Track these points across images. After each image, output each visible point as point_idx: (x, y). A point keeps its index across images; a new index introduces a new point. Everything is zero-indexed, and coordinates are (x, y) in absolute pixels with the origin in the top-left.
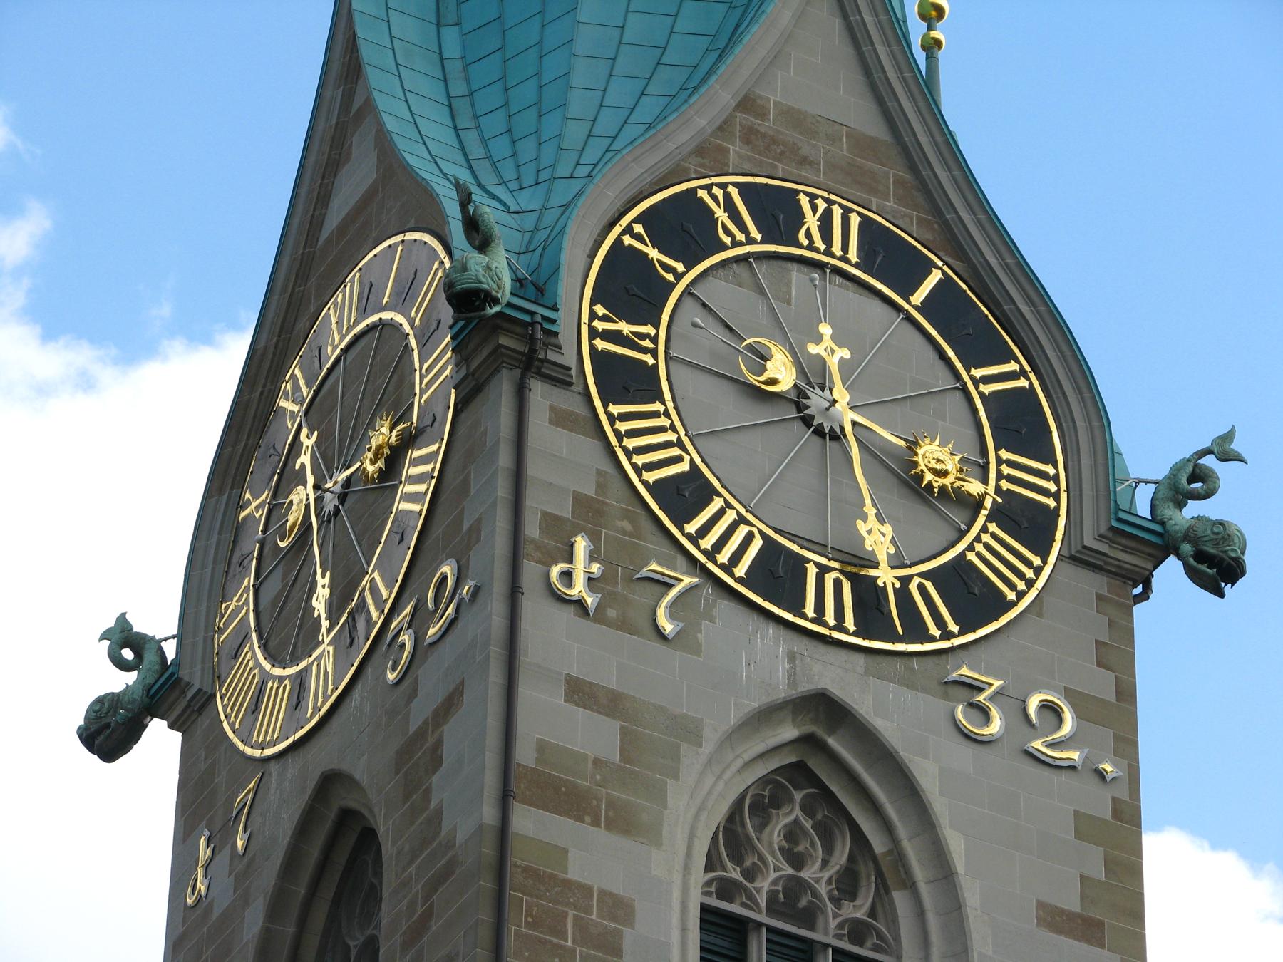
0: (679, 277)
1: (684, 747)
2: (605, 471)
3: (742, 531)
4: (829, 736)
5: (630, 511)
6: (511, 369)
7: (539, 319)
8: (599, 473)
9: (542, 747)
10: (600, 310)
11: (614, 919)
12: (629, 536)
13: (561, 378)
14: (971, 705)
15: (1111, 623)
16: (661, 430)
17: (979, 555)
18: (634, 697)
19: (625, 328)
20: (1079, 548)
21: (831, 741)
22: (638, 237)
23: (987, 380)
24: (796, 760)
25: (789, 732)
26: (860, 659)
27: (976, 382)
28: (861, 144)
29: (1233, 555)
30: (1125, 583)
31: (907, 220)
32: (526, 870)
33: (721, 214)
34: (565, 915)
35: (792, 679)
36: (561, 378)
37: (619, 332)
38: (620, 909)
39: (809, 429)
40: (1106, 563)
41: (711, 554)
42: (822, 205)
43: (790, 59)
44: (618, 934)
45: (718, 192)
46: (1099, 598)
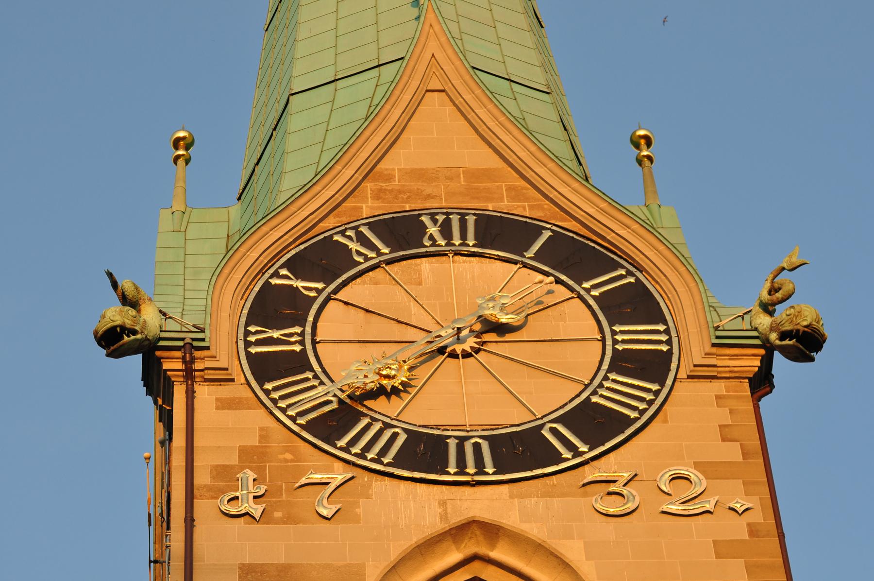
2: (266, 427)
3: (388, 434)
4: (492, 551)
5: (287, 446)
6: (181, 384)
7: (187, 341)
12: (291, 462)
14: (609, 493)
15: (731, 411)
18: (301, 564)
19: (276, 334)
20: (692, 368)
21: (494, 554)
24: (470, 578)
25: (455, 557)
26: (505, 488)
27: (588, 291)
29: (805, 323)
30: (741, 382)
33: (353, 246)
35: (444, 517)
37: (272, 338)
39: (444, 355)
40: (718, 372)
41: (362, 455)
42: (441, 218)
43: (411, 141)
46: (718, 397)
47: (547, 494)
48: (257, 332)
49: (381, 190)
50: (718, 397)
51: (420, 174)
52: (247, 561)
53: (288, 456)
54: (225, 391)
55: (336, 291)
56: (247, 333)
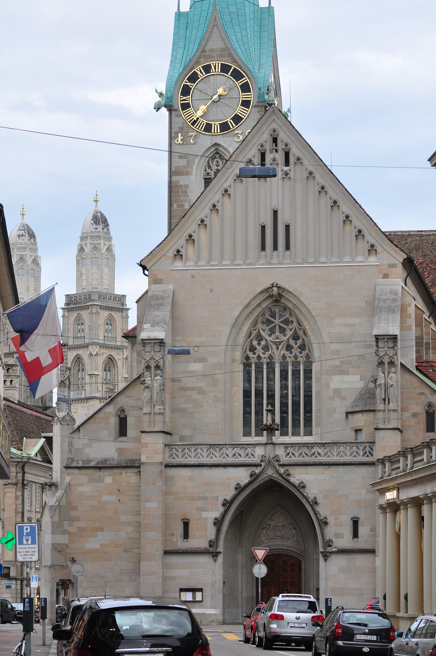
0: (193, 86)
3: (203, 123)
9: (176, 167)
10: (181, 96)
11: (186, 188)
16: (191, 112)
19: (185, 98)
21: (219, 148)
22: (187, 82)
23: (240, 83)
25: (213, 149)
26: (221, 136)
32: (174, 186)
35: (211, 143)
36: (176, 110)
38: (187, 186)
42: (214, 64)
45: (199, 69)
47: (228, 137)
48: (182, 98)
49: (205, 55)
51: (212, 50)
54: (177, 113)
56: (180, 98)
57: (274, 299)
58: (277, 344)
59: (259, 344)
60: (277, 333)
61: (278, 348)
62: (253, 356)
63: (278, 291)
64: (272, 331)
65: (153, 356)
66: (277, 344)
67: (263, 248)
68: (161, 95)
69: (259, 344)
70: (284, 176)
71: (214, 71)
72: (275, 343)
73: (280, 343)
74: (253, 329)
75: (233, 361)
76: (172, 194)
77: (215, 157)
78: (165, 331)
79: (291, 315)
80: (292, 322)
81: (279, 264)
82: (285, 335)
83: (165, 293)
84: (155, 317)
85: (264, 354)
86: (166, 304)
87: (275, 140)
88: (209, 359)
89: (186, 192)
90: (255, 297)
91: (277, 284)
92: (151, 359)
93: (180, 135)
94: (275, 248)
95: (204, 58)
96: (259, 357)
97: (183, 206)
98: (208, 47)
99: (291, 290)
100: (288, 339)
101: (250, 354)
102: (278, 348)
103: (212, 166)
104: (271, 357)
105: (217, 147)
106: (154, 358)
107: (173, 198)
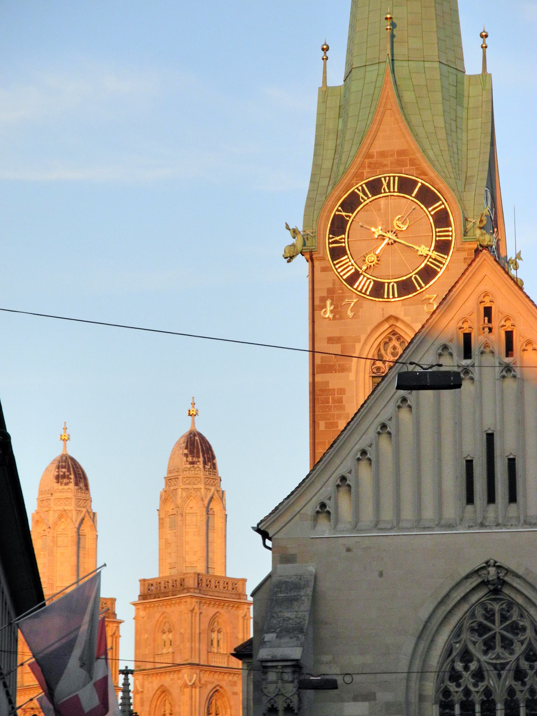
0: (350, 217)
1: (357, 344)
8: (334, 280)
10: (331, 236)
11: (341, 394)
13: (323, 259)
17: (431, 262)
19: (337, 238)
25: (387, 326)
28: (402, 153)
31: (413, 170)
33: (361, 194)
34: (329, 398)
35: (383, 316)
38: (342, 391)
42: (387, 178)
44: (342, 398)
45: (360, 188)
46: (465, 259)
48: (333, 238)
49: (370, 163)
50: (465, 259)
51: (382, 154)
52: (329, 336)
53: (340, 291)
54: (324, 264)
55: (354, 218)
56: (329, 238)
57: (491, 587)
58: (499, 668)
59: (466, 668)
60: (498, 649)
61: (499, 676)
62: (457, 689)
63: (498, 573)
64: (489, 646)
65: (282, 690)
66: (499, 668)
67: (470, 500)
68: (295, 232)
69: (466, 668)
70: (504, 373)
71: (387, 191)
72: (495, 666)
73: (503, 666)
74: (455, 641)
75: (421, 698)
76: (316, 405)
77: (390, 339)
78: (302, 645)
79: (522, 616)
80: (524, 629)
81: (499, 527)
82: (512, 653)
83: (300, 579)
84: (284, 620)
85: (475, 685)
86: (303, 598)
87: (488, 312)
88: (379, 695)
89: (340, 401)
90: (458, 584)
91: (496, 562)
92: (277, 695)
93: (328, 302)
94: (491, 499)
95: (369, 167)
96: (467, 692)
97: (335, 425)
98: (375, 150)
99: (520, 572)
100: (518, 659)
101: (451, 686)
102: (499, 676)
103: (384, 355)
104: (488, 692)
105: (392, 323)
106: (282, 694)
107: (319, 411)
